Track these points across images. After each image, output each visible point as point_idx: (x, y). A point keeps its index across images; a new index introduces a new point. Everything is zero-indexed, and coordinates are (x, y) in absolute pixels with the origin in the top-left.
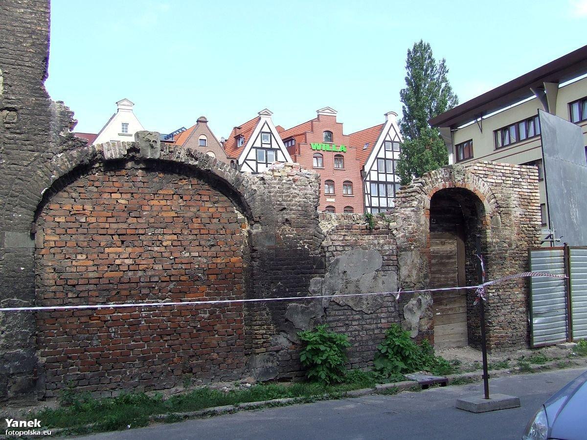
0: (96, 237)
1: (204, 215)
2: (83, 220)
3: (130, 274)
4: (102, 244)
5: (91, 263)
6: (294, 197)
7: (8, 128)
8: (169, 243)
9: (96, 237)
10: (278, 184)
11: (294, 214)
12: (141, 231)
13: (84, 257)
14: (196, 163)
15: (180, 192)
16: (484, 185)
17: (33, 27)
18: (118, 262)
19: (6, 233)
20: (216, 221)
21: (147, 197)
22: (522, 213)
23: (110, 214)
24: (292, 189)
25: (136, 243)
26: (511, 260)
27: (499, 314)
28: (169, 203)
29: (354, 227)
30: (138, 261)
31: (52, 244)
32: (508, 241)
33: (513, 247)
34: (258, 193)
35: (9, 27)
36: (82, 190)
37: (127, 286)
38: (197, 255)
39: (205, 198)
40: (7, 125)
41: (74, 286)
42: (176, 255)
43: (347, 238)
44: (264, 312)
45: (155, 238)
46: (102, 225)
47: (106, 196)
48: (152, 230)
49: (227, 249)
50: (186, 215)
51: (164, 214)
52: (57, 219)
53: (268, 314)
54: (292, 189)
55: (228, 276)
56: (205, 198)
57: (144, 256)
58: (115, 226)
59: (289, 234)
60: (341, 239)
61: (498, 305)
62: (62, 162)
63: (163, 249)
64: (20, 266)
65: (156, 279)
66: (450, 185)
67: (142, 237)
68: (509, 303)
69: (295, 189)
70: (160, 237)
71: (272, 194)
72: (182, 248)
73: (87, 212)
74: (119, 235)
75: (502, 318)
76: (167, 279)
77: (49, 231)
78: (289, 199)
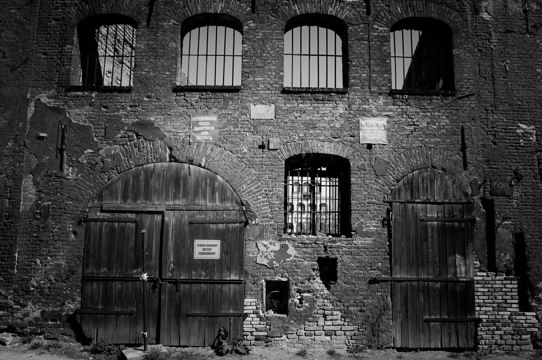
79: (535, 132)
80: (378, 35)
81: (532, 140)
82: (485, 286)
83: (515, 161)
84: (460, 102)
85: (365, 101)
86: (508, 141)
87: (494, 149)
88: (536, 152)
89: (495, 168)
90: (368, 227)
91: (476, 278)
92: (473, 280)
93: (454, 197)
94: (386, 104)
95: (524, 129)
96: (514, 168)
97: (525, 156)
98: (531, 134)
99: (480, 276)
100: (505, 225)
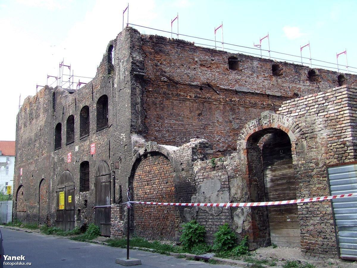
6: (184, 157)
9: (143, 183)
16: (288, 120)
22: (329, 133)
26: (318, 177)
27: (308, 223)
32: (315, 161)
33: (320, 166)
38: (163, 187)
42: (159, 188)
43: (204, 174)
44: (177, 212)
51: (156, 172)
58: (146, 178)
61: (307, 216)
66: (259, 128)
68: (318, 215)
75: (312, 228)
81: (124, 141)
88: (125, 146)
99: (112, 205)
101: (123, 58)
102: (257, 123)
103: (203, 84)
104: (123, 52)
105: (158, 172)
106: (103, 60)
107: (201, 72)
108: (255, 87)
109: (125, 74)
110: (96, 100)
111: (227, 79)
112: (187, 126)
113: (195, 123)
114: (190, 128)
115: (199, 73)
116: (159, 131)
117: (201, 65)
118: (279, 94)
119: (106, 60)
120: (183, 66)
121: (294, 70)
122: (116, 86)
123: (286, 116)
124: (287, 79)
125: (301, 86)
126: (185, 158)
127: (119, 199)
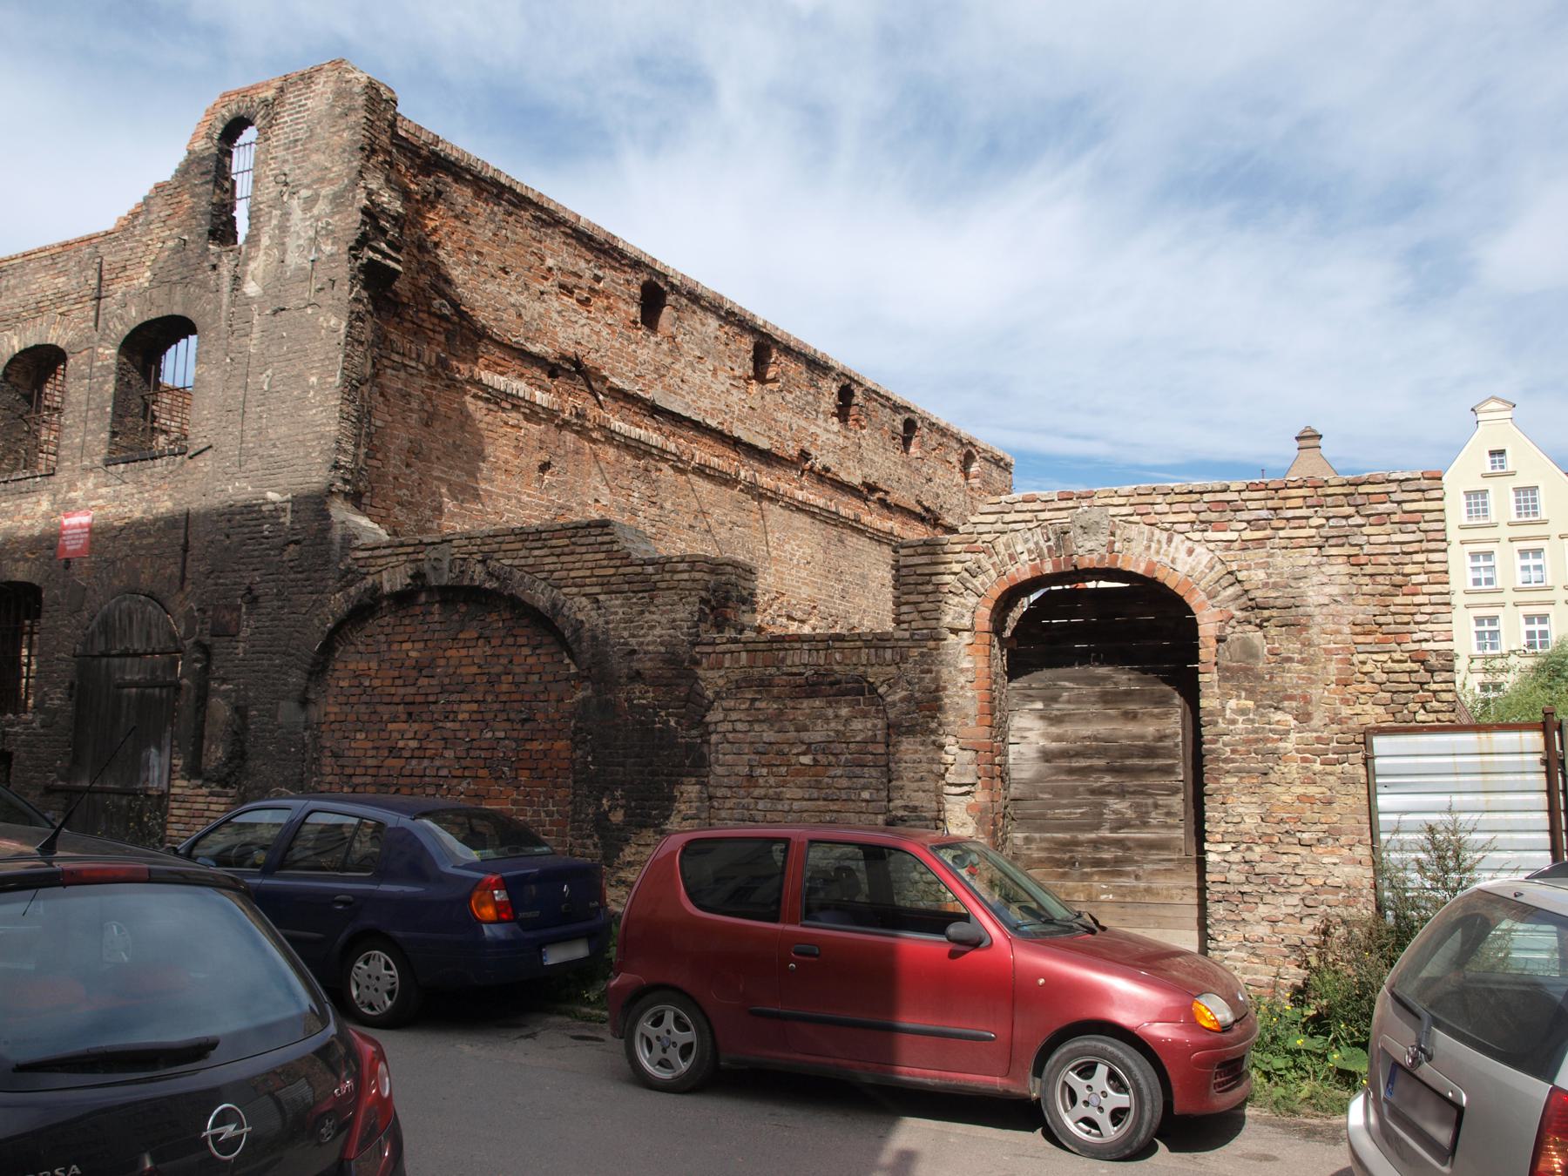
0: (380, 708)
1: (517, 670)
2: (367, 684)
3: (414, 762)
4: (385, 717)
5: (370, 745)
6: (652, 628)
7: (292, 568)
8: (466, 716)
9: (380, 708)
10: (622, 606)
11: (651, 660)
12: (431, 699)
13: (364, 735)
14: (495, 585)
15: (487, 633)
16: (1190, 552)
17: (322, 429)
18: (401, 744)
19: (282, 703)
20: (535, 678)
21: (444, 645)
22: (1360, 618)
23: (396, 674)
24: (647, 614)
25: (424, 717)
26: (1305, 760)
27: (1246, 915)
28: (471, 652)
29: (777, 680)
30: (425, 744)
31: (332, 718)
32: (1294, 704)
33: (1316, 722)
34: (587, 625)
35: (300, 438)
36: (370, 641)
37: (408, 780)
38: (502, 735)
39: (522, 640)
40: (292, 564)
41: (350, 776)
42: (476, 735)
43: (758, 704)
44: (589, 842)
45: (449, 708)
46: (387, 690)
47: (395, 647)
48: (446, 695)
49: (548, 726)
50: (492, 671)
51: (464, 671)
52: (342, 684)
53: (595, 846)
54: (647, 614)
55: (548, 773)
56: (522, 640)
57: (433, 735)
58: (402, 691)
59: (639, 698)
60: (743, 707)
61: (1245, 888)
62: (338, 603)
63: (457, 726)
64: (291, 746)
65: (444, 772)
66: (1056, 564)
67: (432, 707)
68: (1292, 890)
69: (653, 613)
70: (455, 707)
71: (611, 626)
72: (483, 725)
73: (372, 673)
74: (406, 704)
75: (1263, 930)
76: (459, 773)
77: (331, 700)
78: (642, 632)
79: (289, 505)
80: (102, 366)
81: (283, 523)
82: (184, 805)
83: (251, 567)
84: (191, 464)
85: (72, 486)
86: (246, 530)
87: (227, 549)
88: (288, 544)
89: (222, 585)
90: (51, 699)
91: (173, 791)
92: (169, 794)
93: (159, 643)
94: (96, 486)
95: (274, 503)
96: (247, 581)
97: (269, 555)
98: (284, 510)
99: (181, 786)
100: (225, 691)
101: (314, 182)
102: (1051, 543)
103: (563, 357)
104: (314, 157)
105: (474, 669)
106: (184, 172)
107: (559, 312)
108: (705, 403)
109: (319, 250)
110: (121, 330)
111: (633, 358)
112: (502, 500)
113: (529, 495)
114: (510, 512)
115: (555, 316)
116: (410, 503)
117: (562, 286)
118: (763, 444)
119: (203, 174)
120: (507, 273)
121: (805, 375)
122: (251, 288)
123: (1182, 537)
124: (789, 397)
125: (819, 431)
126: (658, 631)
127: (225, 765)
